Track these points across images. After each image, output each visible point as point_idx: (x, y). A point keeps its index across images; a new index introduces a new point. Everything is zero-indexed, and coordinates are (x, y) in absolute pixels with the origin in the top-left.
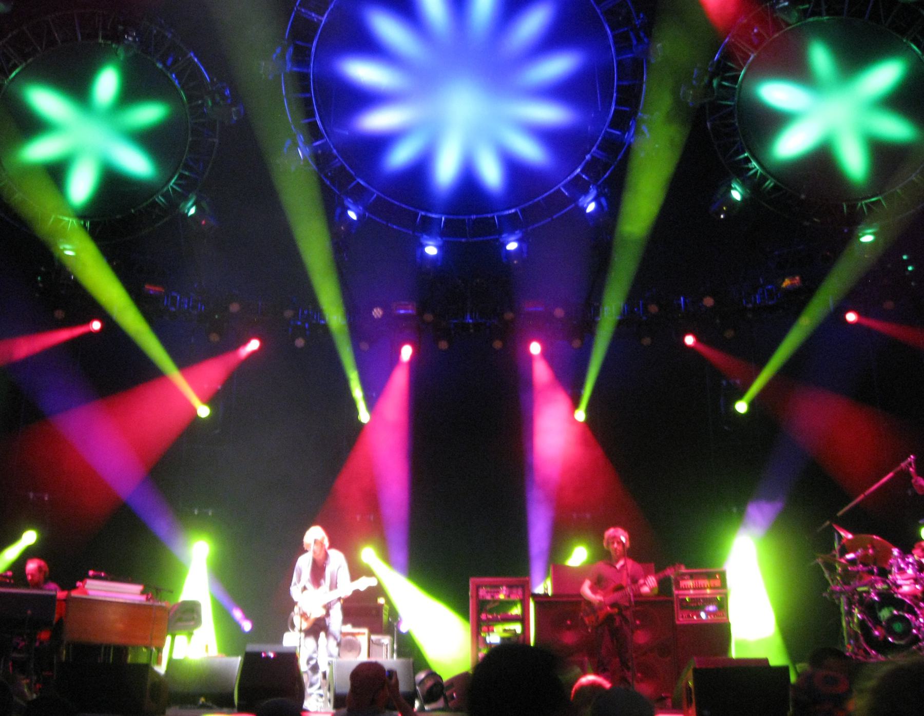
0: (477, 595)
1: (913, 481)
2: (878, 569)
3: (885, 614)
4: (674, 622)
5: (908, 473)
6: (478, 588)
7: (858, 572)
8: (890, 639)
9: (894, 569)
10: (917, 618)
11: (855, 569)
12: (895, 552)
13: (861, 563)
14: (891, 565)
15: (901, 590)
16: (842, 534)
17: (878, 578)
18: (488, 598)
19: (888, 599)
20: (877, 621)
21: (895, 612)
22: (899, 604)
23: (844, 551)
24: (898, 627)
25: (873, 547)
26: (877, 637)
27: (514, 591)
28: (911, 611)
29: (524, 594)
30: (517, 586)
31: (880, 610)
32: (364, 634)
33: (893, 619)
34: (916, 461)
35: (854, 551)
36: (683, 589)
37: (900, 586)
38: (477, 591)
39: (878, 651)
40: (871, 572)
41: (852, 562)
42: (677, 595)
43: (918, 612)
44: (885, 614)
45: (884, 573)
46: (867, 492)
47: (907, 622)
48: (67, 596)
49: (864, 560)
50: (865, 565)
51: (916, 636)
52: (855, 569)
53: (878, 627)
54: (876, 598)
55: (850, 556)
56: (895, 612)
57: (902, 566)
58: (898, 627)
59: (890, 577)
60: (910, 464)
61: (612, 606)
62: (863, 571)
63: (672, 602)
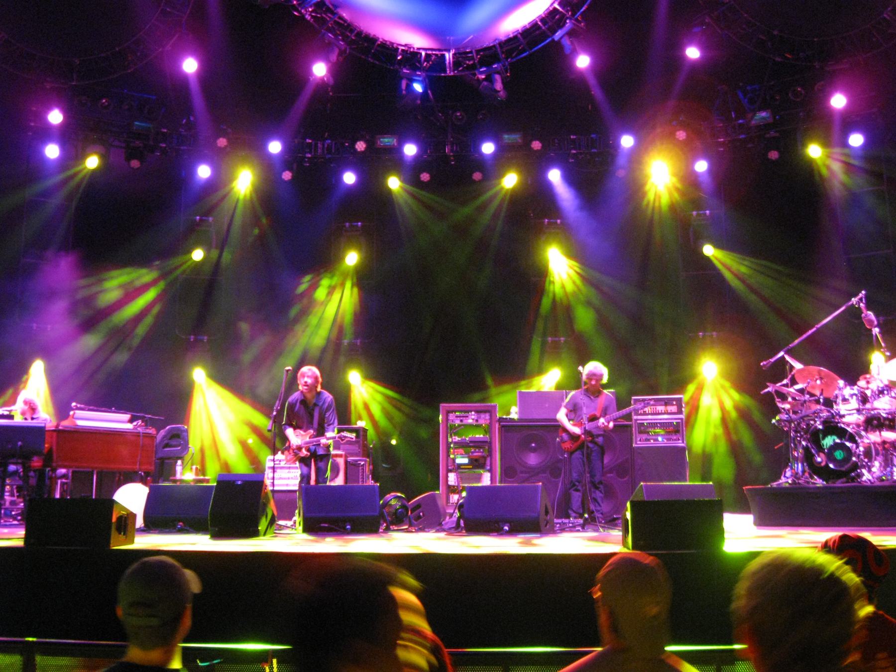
1: (863, 315)
2: (825, 399)
3: (829, 441)
5: (859, 308)
7: (805, 401)
8: (831, 466)
9: (839, 400)
10: (857, 447)
11: (803, 398)
14: (837, 397)
15: (844, 420)
17: (823, 408)
19: (832, 427)
20: (820, 449)
21: (838, 441)
22: (842, 433)
23: (793, 382)
25: (821, 379)
26: (820, 463)
27: (483, 416)
28: (852, 438)
29: (491, 419)
30: (485, 412)
31: (824, 438)
32: (340, 456)
33: (835, 447)
34: (866, 296)
36: (641, 414)
37: (843, 416)
39: (820, 477)
40: (817, 402)
42: (636, 420)
43: (859, 441)
44: (829, 441)
45: (829, 403)
53: (821, 454)
56: (838, 441)
57: (847, 397)
58: (839, 455)
59: (835, 407)
62: (810, 401)
63: (631, 426)
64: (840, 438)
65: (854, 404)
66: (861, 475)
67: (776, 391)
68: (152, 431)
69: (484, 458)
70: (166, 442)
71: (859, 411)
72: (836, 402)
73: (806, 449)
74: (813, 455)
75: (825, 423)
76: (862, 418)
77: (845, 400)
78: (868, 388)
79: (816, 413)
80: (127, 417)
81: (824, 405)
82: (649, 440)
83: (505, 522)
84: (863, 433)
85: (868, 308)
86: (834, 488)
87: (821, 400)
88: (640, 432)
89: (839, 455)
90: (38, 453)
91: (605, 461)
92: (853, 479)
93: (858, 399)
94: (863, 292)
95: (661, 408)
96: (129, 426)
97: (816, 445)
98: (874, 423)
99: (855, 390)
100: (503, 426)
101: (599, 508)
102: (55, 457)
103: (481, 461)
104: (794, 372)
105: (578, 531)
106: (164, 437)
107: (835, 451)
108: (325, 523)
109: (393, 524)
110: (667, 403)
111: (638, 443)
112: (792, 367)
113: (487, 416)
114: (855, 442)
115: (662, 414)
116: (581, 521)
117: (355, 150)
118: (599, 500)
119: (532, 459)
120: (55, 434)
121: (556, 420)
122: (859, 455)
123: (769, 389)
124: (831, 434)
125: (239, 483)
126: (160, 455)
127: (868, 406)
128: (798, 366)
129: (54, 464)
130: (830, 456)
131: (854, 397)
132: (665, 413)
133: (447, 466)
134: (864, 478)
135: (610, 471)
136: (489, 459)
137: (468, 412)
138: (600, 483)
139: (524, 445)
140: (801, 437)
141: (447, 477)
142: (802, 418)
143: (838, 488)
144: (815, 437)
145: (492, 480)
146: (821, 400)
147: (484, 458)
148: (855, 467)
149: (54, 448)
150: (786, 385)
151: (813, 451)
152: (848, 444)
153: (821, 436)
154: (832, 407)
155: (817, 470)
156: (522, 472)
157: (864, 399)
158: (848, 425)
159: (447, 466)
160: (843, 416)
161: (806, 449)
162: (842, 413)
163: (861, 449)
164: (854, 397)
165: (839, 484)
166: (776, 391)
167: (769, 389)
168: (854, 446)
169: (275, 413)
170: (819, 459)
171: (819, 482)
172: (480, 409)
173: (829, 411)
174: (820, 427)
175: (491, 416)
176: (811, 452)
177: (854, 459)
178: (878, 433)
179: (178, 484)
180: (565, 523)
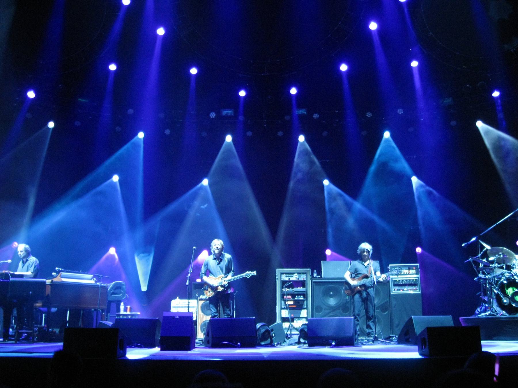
0: (281, 278)
2: (507, 266)
6: (282, 274)
7: (495, 267)
8: (514, 305)
11: (493, 266)
13: (496, 263)
16: (484, 245)
17: (506, 271)
18: (287, 279)
20: (506, 295)
25: (503, 254)
26: (506, 303)
30: (303, 273)
31: (507, 289)
35: (494, 255)
40: (502, 268)
42: (392, 278)
44: (510, 291)
45: (509, 268)
48: (52, 281)
50: (499, 264)
52: (493, 266)
54: (505, 282)
55: (491, 259)
61: (361, 286)
63: (389, 282)
67: (474, 261)
69: (303, 301)
74: (502, 299)
75: (508, 279)
79: (502, 274)
80: (91, 276)
81: (506, 269)
82: (399, 290)
83: (333, 339)
87: (504, 267)
88: (395, 285)
95: (406, 271)
96: (92, 282)
97: (502, 292)
100: (314, 282)
104: (485, 249)
105: (371, 344)
106: (112, 288)
110: (410, 268)
111: (394, 291)
112: (483, 247)
113: (305, 276)
115: (407, 274)
116: (372, 338)
117: (210, 117)
119: (332, 302)
120: (50, 286)
121: (344, 278)
123: (470, 259)
125: (177, 317)
126: (109, 299)
128: (487, 247)
130: (512, 299)
132: (408, 274)
135: (377, 309)
136: (305, 302)
138: (372, 316)
139: (326, 294)
140: (495, 288)
142: (494, 277)
144: (503, 288)
146: (504, 267)
151: (502, 296)
156: (325, 309)
161: (497, 295)
169: (189, 275)
170: (505, 301)
171: (503, 314)
172: (298, 272)
173: (510, 273)
174: (505, 282)
175: (307, 276)
180: (362, 340)
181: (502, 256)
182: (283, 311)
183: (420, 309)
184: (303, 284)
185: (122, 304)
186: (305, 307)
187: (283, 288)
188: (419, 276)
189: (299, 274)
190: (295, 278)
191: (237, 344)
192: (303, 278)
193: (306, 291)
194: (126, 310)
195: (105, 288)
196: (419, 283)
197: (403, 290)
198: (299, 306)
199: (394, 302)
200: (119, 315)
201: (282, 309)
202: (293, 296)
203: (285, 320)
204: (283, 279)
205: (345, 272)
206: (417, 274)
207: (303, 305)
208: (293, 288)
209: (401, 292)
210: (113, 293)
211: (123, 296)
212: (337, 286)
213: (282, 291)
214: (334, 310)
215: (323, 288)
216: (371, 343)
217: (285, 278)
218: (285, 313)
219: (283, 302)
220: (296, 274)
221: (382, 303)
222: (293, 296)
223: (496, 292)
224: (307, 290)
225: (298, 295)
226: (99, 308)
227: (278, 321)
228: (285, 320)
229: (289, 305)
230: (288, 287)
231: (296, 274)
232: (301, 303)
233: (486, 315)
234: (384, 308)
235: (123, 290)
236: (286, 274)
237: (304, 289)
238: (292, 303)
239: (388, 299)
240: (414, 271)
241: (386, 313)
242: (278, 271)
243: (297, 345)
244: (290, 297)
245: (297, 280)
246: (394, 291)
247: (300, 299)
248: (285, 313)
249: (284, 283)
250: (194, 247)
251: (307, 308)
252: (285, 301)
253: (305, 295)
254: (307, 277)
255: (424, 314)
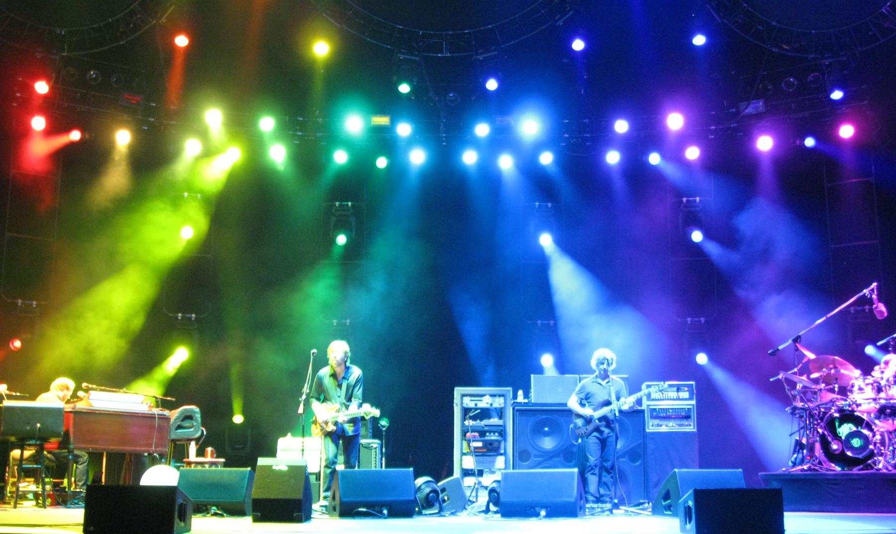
0: (462, 403)
2: (840, 388)
4: (644, 429)
5: (871, 298)
6: (463, 396)
7: (821, 390)
8: (849, 454)
9: (856, 389)
10: (874, 436)
11: (818, 387)
12: (857, 373)
14: (853, 386)
15: (860, 408)
17: (839, 397)
19: (848, 416)
20: (836, 437)
21: (854, 429)
22: (858, 421)
24: (856, 443)
26: (836, 450)
28: (869, 426)
30: (500, 396)
31: (840, 426)
33: (852, 435)
34: (878, 287)
35: (819, 369)
36: (653, 400)
37: (858, 405)
38: (462, 400)
40: (832, 391)
41: (816, 381)
42: (648, 406)
43: (875, 429)
44: (845, 430)
45: (844, 391)
46: (829, 316)
47: (865, 438)
49: (827, 380)
50: (827, 384)
51: (872, 451)
52: (818, 387)
55: (815, 375)
56: (854, 429)
57: (863, 386)
59: (851, 396)
60: (872, 290)
64: (857, 425)
65: (869, 393)
66: (874, 463)
68: (166, 413)
69: (499, 442)
70: (179, 423)
71: (875, 400)
72: (851, 391)
73: (823, 437)
74: (830, 443)
76: (873, 406)
77: (861, 389)
78: (882, 378)
79: (832, 402)
82: (659, 425)
83: (543, 507)
84: (877, 422)
85: (880, 300)
86: (852, 474)
87: (836, 389)
88: (653, 417)
89: (856, 443)
90: (57, 435)
91: (619, 446)
92: (869, 467)
93: (873, 389)
94: (875, 284)
95: (674, 394)
97: (831, 432)
98: (889, 411)
99: (870, 380)
100: (518, 410)
101: (608, 493)
102: (72, 439)
103: (496, 445)
106: (178, 418)
107: (853, 438)
108: (363, 507)
109: (424, 508)
111: (652, 427)
112: (804, 356)
113: (502, 400)
114: (871, 430)
118: (610, 484)
119: (548, 443)
122: (875, 444)
123: (780, 376)
124: (848, 421)
127: (882, 395)
129: (71, 446)
131: (870, 387)
133: (462, 449)
134: (880, 466)
135: (623, 456)
136: (503, 443)
137: (482, 396)
139: (538, 430)
140: (818, 425)
141: (461, 460)
143: (858, 475)
144: (831, 426)
145: (506, 463)
146: (836, 389)
147: (499, 442)
148: (872, 455)
149: (71, 431)
150: (795, 373)
151: (830, 439)
152: (866, 432)
153: (837, 424)
154: (847, 396)
155: (831, 456)
156: (536, 456)
157: (879, 390)
158: (862, 412)
159: (462, 449)
160: (860, 405)
161: (823, 437)
162: (858, 402)
163: (878, 437)
164: (870, 387)
165: (855, 471)
166: (786, 379)
167: (780, 376)
168: (871, 435)
170: (835, 447)
174: (837, 415)
175: (505, 400)
176: (827, 440)
177: (871, 447)
178: (891, 421)
179: (193, 465)
180: (593, 508)
181: (833, 371)
182: (464, 457)
183: (695, 455)
184: (501, 413)
185: (193, 444)
186: (502, 451)
187: (465, 420)
188: (694, 402)
189: (493, 396)
190: (485, 402)
191: (381, 512)
192: (498, 403)
193: (504, 426)
194: (201, 452)
195: (167, 419)
196: (694, 415)
197: (667, 426)
198: (491, 450)
199: (651, 446)
200: (189, 463)
201: (463, 454)
202: (482, 433)
203: (467, 473)
204: (465, 405)
205: (569, 396)
206: (691, 399)
207: (499, 448)
208: (481, 420)
209: (664, 429)
210: (180, 427)
211: (196, 431)
212: (555, 417)
213: (463, 425)
214: (550, 459)
215: (532, 420)
216: (608, 513)
217: (469, 403)
218: (469, 462)
219: (465, 444)
220: (488, 397)
221: (631, 446)
222: (482, 433)
223: (820, 431)
224: (505, 422)
225: (490, 432)
226: (156, 452)
227: (457, 474)
228: (467, 473)
229: (475, 448)
230: (474, 418)
231: (488, 397)
232: (496, 445)
233: (803, 470)
234: (633, 454)
235: (196, 421)
236: (471, 395)
237: (501, 422)
238: (480, 444)
239: (641, 441)
240: (686, 395)
241: (637, 464)
242: (458, 391)
243: (483, 514)
244: (476, 434)
245: (488, 406)
246: (652, 427)
247: (493, 438)
248: (469, 462)
249: (466, 411)
250: (314, 351)
251: (505, 454)
252: (469, 442)
253: (502, 433)
254: (505, 403)
255: (701, 467)
